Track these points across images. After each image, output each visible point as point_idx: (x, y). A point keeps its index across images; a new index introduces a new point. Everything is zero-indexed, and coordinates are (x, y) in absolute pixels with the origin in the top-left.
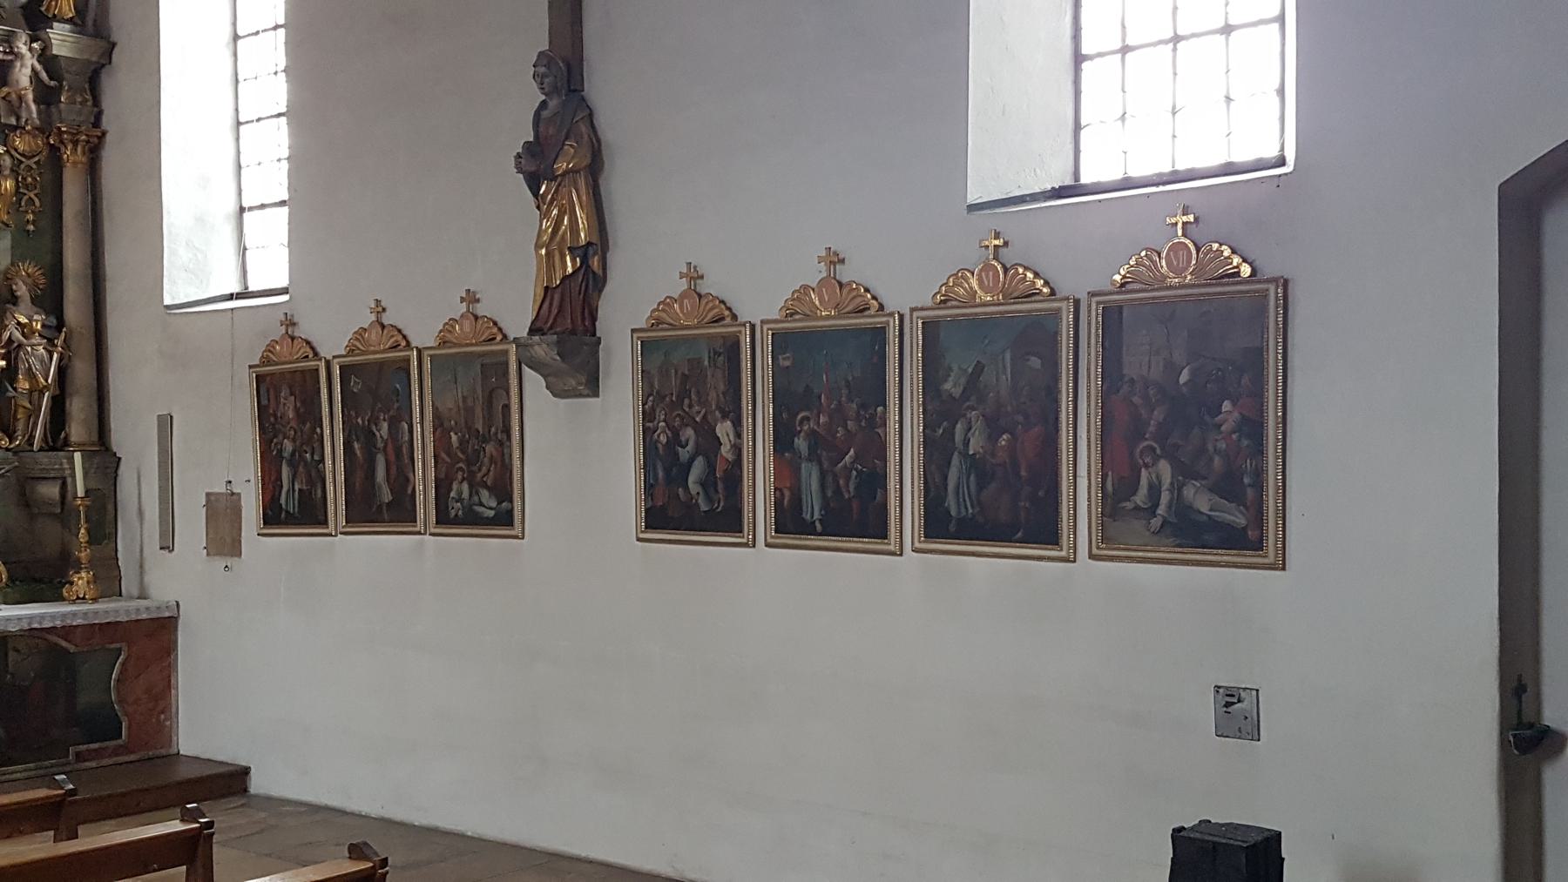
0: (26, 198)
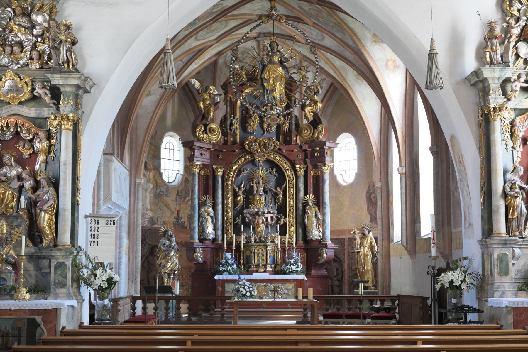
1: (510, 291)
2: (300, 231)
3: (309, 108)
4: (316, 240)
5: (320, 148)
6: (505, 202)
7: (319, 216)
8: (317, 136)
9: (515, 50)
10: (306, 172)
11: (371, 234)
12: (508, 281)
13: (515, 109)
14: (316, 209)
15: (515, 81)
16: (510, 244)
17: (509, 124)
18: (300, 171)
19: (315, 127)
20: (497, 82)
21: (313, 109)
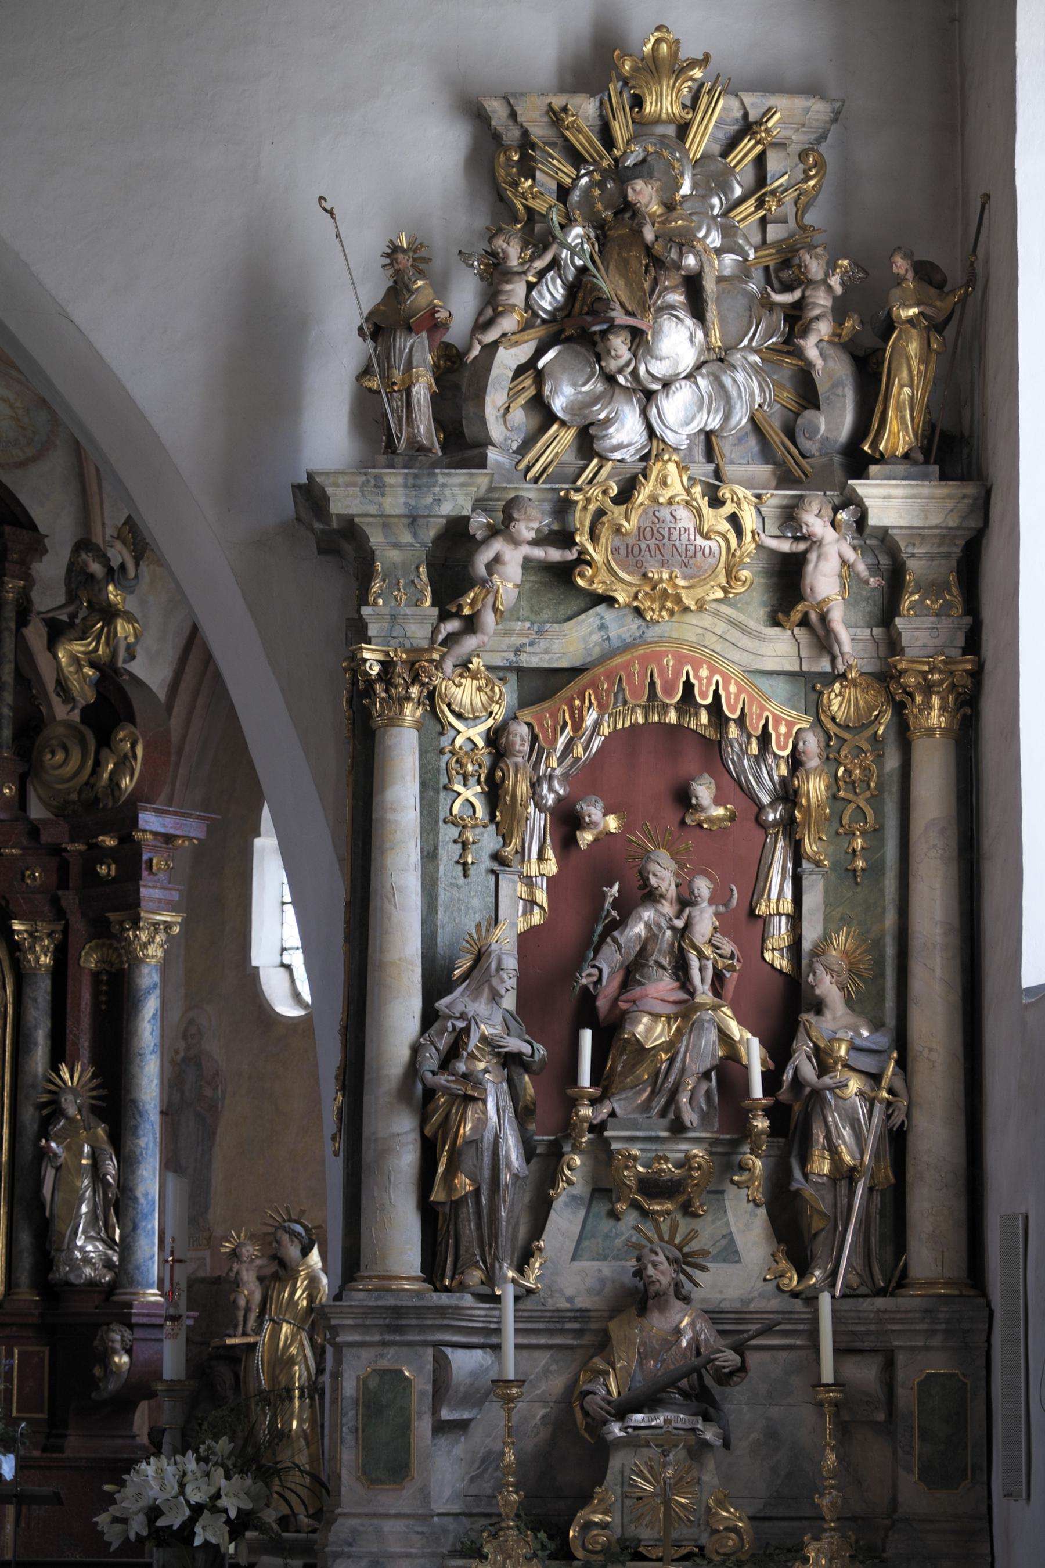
0: (853, 806)
1: (408, 1555)
2: (25, 1239)
3: (78, 647)
4: (91, 1283)
5: (121, 841)
6: (424, 1121)
7: (111, 1167)
8: (111, 778)
9: (528, 382)
10: (61, 954)
11: (315, 1257)
12: (407, 1510)
13: (521, 672)
14: (95, 1135)
15: (494, 532)
16: (423, 1329)
17: (481, 743)
18: (32, 948)
19: (105, 741)
20: (407, 538)
21: (96, 649)
